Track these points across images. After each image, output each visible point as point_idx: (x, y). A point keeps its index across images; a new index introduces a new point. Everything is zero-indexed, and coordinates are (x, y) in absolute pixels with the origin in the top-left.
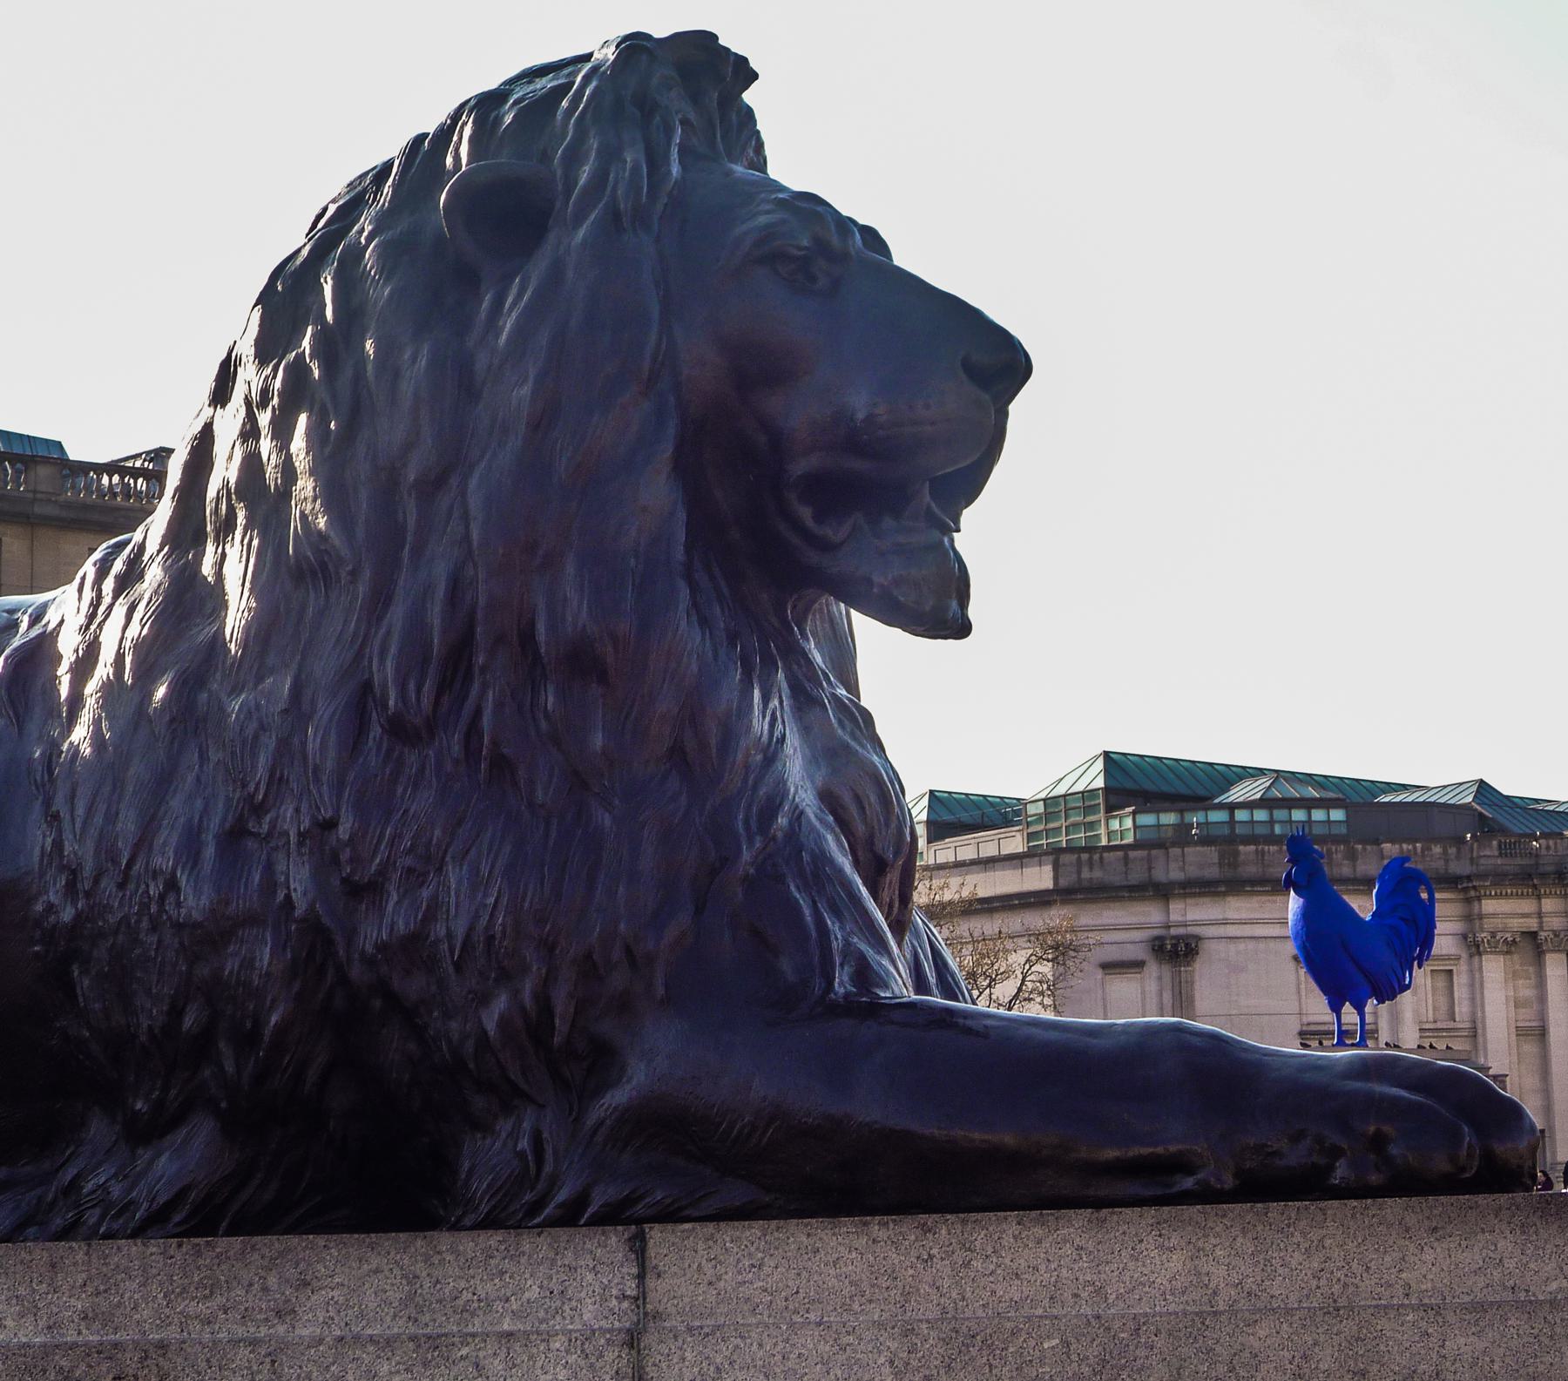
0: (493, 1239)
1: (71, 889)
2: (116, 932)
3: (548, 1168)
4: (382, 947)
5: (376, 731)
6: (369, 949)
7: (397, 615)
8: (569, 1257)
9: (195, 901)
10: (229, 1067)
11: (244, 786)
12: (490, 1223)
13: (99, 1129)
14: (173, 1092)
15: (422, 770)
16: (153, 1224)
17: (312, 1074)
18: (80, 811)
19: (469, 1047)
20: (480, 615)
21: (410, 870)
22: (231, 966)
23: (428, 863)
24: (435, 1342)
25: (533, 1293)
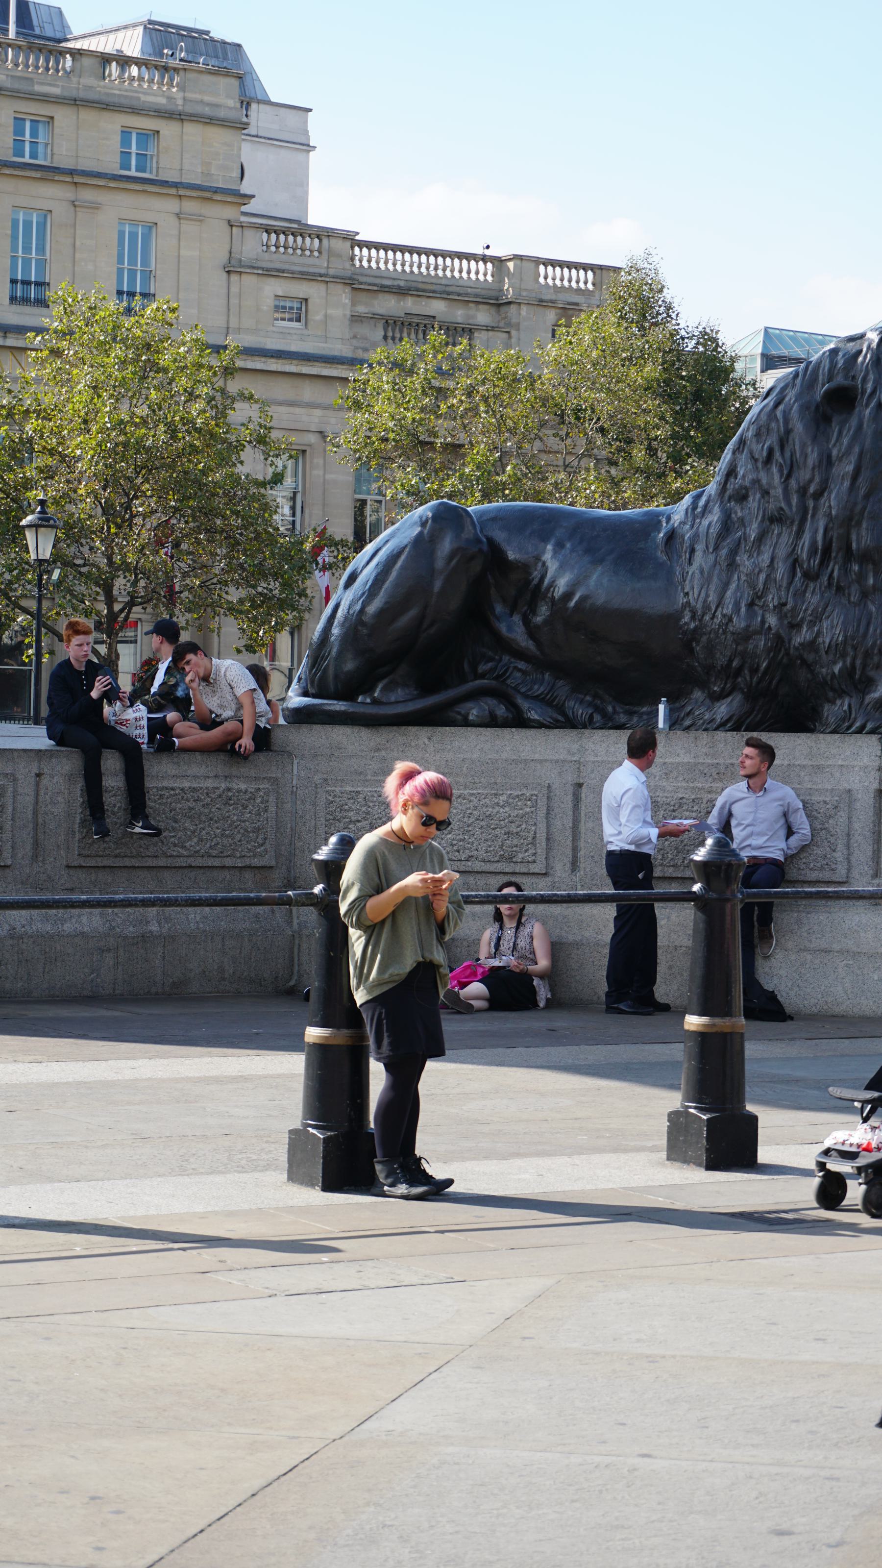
0: (836, 736)
1: (693, 618)
2: (710, 633)
3: (853, 716)
4: (801, 644)
5: (799, 575)
6: (797, 645)
7: (807, 538)
8: (860, 743)
9: (739, 623)
10: (748, 678)
11: (754, 589)
12: (834, 732)
13: (698, 694)
14: (728, 685)
15: (814, 589)
16: (721, 726)
17: (774, 682)
18: (696, 591)
19: (829, 677)
20: (834, 540)
21: (811, 621)
22: (750, 647)
23: (817, 617)
24: (818, 767)
25: (848, 753)
